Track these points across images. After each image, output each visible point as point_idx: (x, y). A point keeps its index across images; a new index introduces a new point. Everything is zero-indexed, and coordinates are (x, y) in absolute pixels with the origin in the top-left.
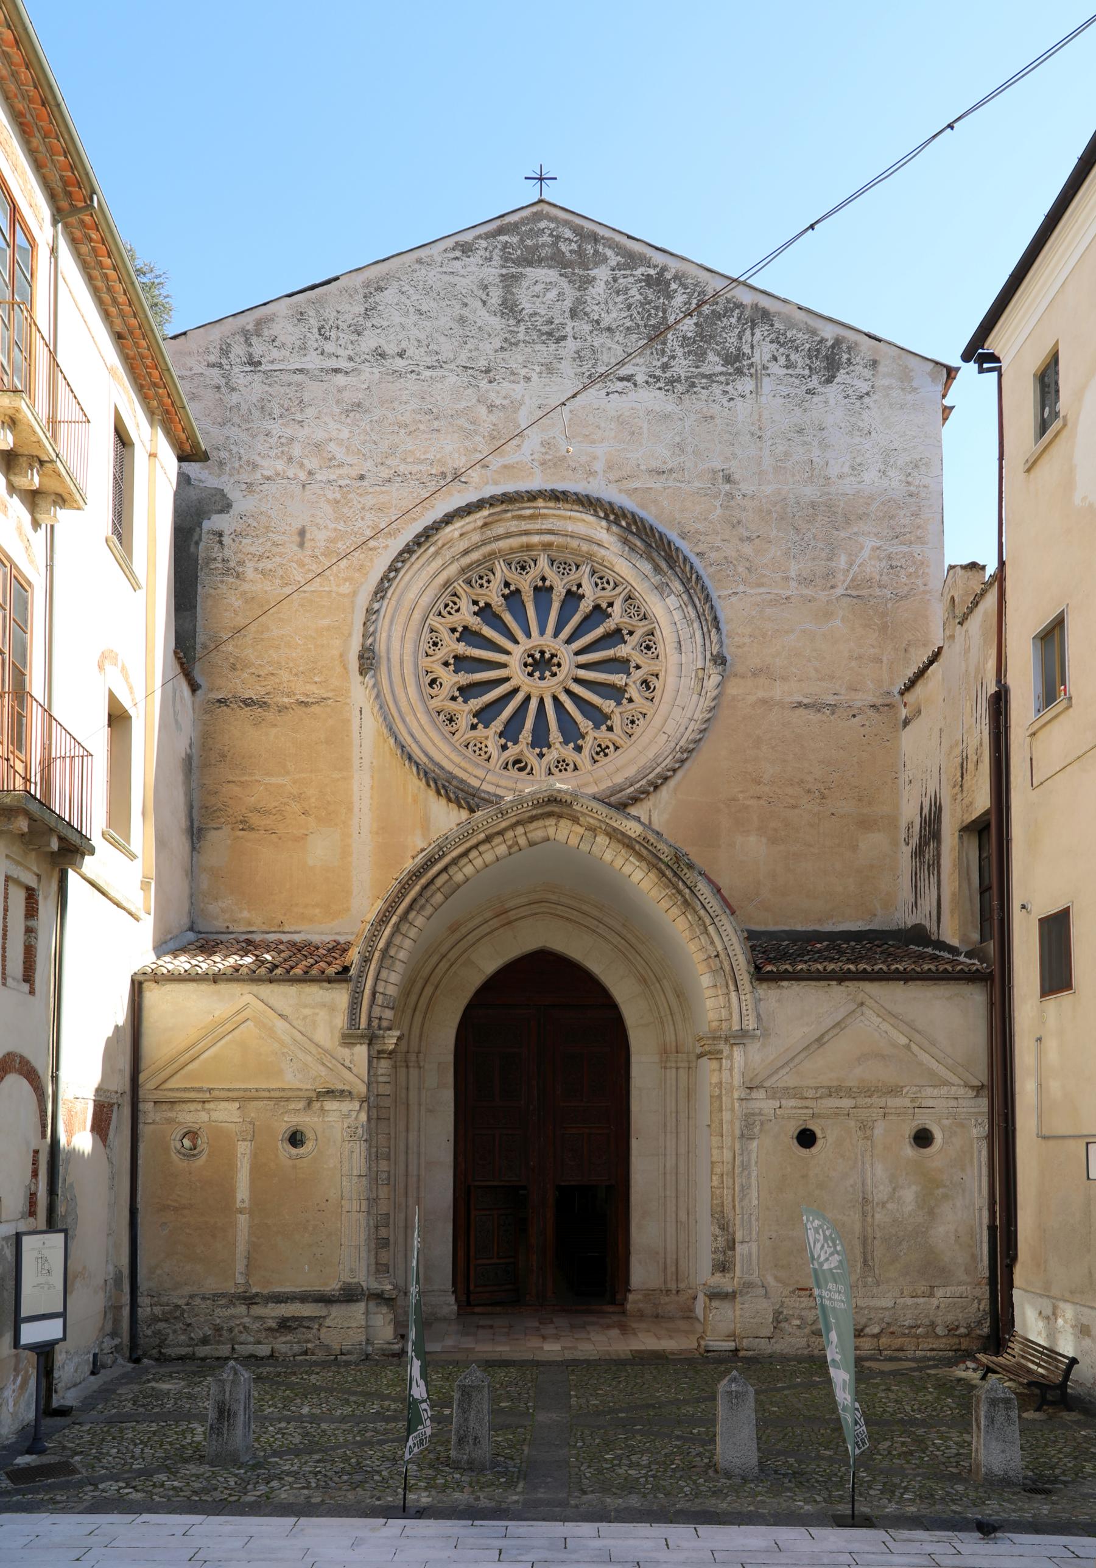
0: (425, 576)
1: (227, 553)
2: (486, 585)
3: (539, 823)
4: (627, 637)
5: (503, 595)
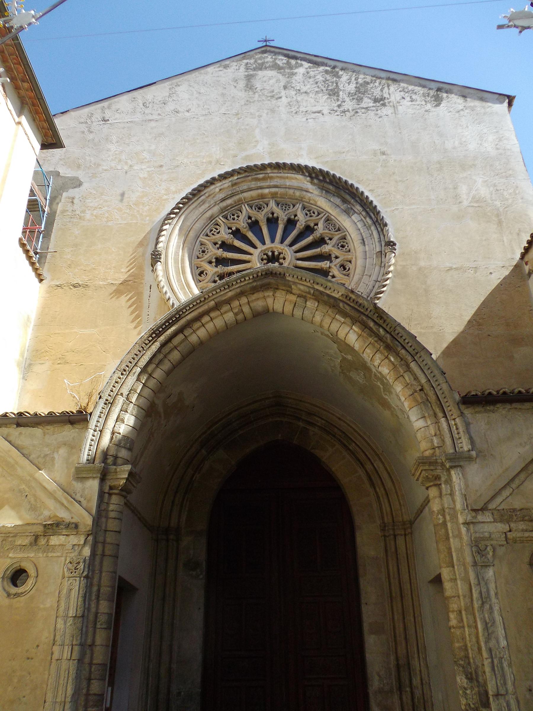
0: (197, 212)
1: (75, 207)
2: (236, 218)
3: (261, 295)
4: (328, 241)
5: (248, 223)
